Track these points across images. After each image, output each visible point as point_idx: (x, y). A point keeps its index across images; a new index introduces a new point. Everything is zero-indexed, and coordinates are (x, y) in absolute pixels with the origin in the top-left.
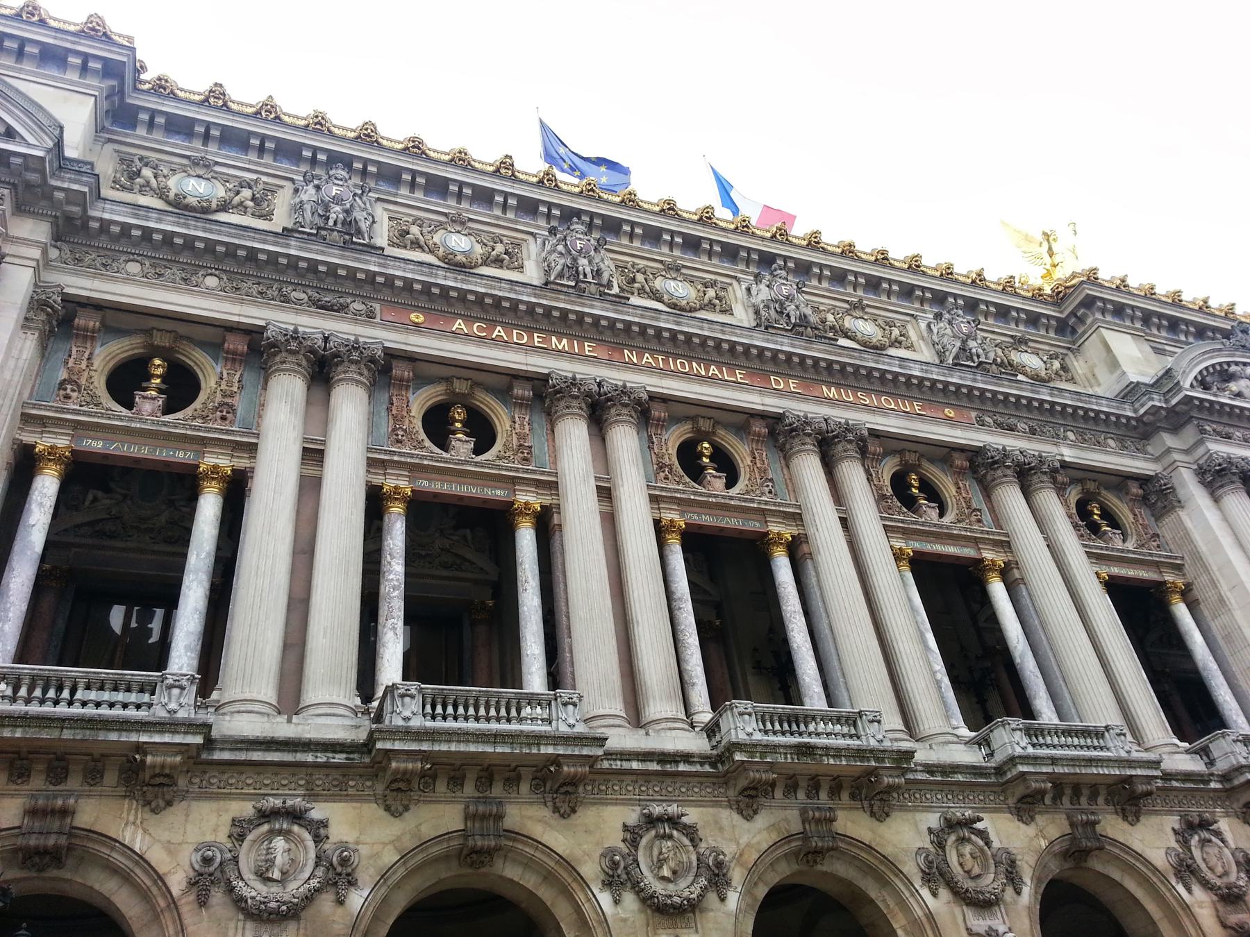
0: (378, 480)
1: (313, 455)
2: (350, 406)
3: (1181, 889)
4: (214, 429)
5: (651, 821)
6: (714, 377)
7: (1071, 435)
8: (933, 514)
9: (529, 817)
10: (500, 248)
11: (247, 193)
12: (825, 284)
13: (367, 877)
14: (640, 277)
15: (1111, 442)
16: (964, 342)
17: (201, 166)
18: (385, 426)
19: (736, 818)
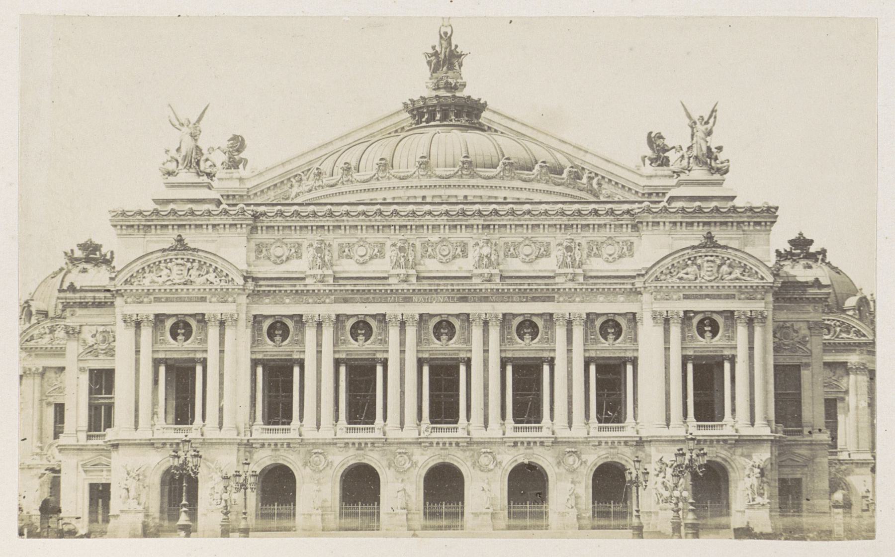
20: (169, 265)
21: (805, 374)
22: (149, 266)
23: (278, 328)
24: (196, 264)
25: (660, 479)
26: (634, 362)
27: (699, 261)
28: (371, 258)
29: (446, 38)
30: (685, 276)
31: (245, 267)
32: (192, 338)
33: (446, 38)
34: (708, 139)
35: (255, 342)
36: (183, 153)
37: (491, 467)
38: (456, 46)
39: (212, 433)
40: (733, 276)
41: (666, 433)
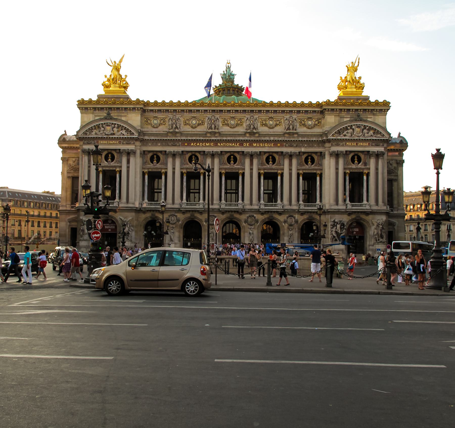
0: (182, 171)
1: (174, 169)
2: (178, 162)
3: (284, 224)
7: (306, 145)
8: (271, 165)
9: (197, 215)
10: (200, 122)
11: (162, 121)
13: (181, 220)
14: (226, 121)
15: (315, 145)
16: (290, 126)
17: (156, 118)
18: (183, 161)
19: (221, 215)
20: (104, 125)
21: (395, 184)
22: (94, 126)
23: (155, 157)
24: (116, 126)
25: (334, 230)
26: (321, 176)
27: (353, 127)
30: (347, 134)
31: (139, 128)
32: (115, 161)
34: (355, 73)
35: (144, 163)
37: (253, 223)
40: (369, 134)
41: (336, 207)
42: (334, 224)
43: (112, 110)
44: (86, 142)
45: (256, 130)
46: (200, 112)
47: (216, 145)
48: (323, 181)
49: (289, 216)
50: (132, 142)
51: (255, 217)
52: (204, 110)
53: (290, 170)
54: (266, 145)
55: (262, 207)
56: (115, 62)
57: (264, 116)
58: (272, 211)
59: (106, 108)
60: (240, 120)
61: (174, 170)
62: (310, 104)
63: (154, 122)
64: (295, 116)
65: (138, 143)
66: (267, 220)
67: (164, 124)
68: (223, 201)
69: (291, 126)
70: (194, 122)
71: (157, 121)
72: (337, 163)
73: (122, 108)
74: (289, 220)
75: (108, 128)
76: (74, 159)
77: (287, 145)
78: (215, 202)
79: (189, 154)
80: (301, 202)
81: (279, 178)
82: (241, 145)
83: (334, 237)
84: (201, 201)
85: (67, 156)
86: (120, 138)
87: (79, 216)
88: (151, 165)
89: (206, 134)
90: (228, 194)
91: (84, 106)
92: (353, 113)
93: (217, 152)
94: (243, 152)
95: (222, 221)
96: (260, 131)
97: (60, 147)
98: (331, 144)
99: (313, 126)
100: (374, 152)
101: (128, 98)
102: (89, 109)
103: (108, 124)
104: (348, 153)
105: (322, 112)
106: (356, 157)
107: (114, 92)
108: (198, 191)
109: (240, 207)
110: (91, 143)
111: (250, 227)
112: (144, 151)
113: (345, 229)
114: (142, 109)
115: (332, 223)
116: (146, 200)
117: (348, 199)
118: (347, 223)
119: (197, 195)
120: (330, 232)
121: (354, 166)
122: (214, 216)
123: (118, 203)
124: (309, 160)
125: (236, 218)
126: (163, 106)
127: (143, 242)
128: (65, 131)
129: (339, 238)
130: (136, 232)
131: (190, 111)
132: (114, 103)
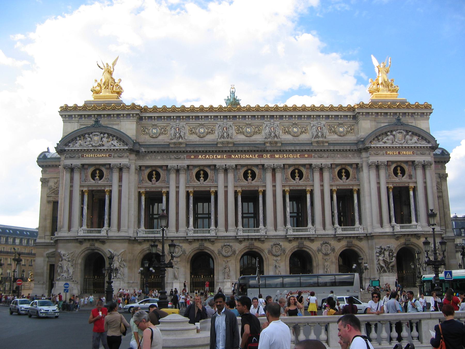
0: (188, 190)
1: (178, 187)
3: (317, 253)
4: (163, 185)
5: (225, 245)
6: (251, 158)
7: (339, 156)
11: (163, 130)
12: (287, 119)
14: (240, 129)
15: (350, 156)
17: (155, 126)
18: (189, 179)
23: (154, 174)
24: (106, 135)
25: (381, 258)
26: (358, 192)
27: (394, 133)
28: (207, 134)
29: (233, 93)
30: (387, 141)
31: (134, 138)
33: (233, 93)
35: (141, 181)
36: (103, 81)
37: (279, 253)
38: (237, 97)
39: (113, 233)
40: (413, 141)
42: (381, 251)
43: (101, 118)
44: (67, 156)
45: (277, 138)
46: (209, 118)
47: (230, 157)
48: (362, 199)
49: (324, 243)
50: (126, 155)
51: (281, 246)
52: (214, 116)
53: (322, 186)
54: (291, 156)
55: (290, 232)
56: (107, 64)
57: (286, 122)
58: (301, 238)
59: (94, 115)
60: (258, 127)
61: (178, 189)
62: (341, 108)
63: (152, 131)
64: (323, 122)
65: (133, 156)
66: (296, 250)
67: (165, 134)
68: (240, 227)
69: (320, 133)
70: (202, 130)
71: (157, 130)
72: (378, 176)
73: (114, 114)
74: (323, 248)
75: (96, 138)
76: (56, 180)
77: (316, 156)
78: (230, 228)
79: (196, 170)
80: (337, 225)
81: (308, 196)
82: (261, 157)
83: (382, 267)
84: (213, 227)
85: (47, 176)
86: (111, 149)
87: (57, 249)
88: (149, 184)
89: (217, 144)
90: (244, 219)
91: (67, 113)
92: (392, 117)
93: (231, 167)
94: (263, 165)
95: (240, 252)
96: (282, 139)
97: (40, 166)
98: (368, 153)
99: (345, 133)
100: (419, 162)
101: (121, 102)
102: (73, 116)
103: (96, 133)
104: (389, 163)
105: (355, 117)
106: (399, 169)
107: (104, 97)
108: (207, 216)
109: (262, 233)
110: (74, 157)
111: (275, 258)
112: (140, 167)
113: (395, 257)
114: (138, 116)
115: (379, 250)
116: (143, 228)
117: (393, 219)
118: (395, 250)
119: (206, 221)
120: (376, 262)
121: (396, 180)
122: (229, 245)
123: (107, 231)
124: (343, 174)
125: (257, 248)
126: (164, 112)
127: (139, 282)
128: (48, 149)
129: (388, 268)
130: (129, 268)
131: (197, 118)
132: (104, 109)
